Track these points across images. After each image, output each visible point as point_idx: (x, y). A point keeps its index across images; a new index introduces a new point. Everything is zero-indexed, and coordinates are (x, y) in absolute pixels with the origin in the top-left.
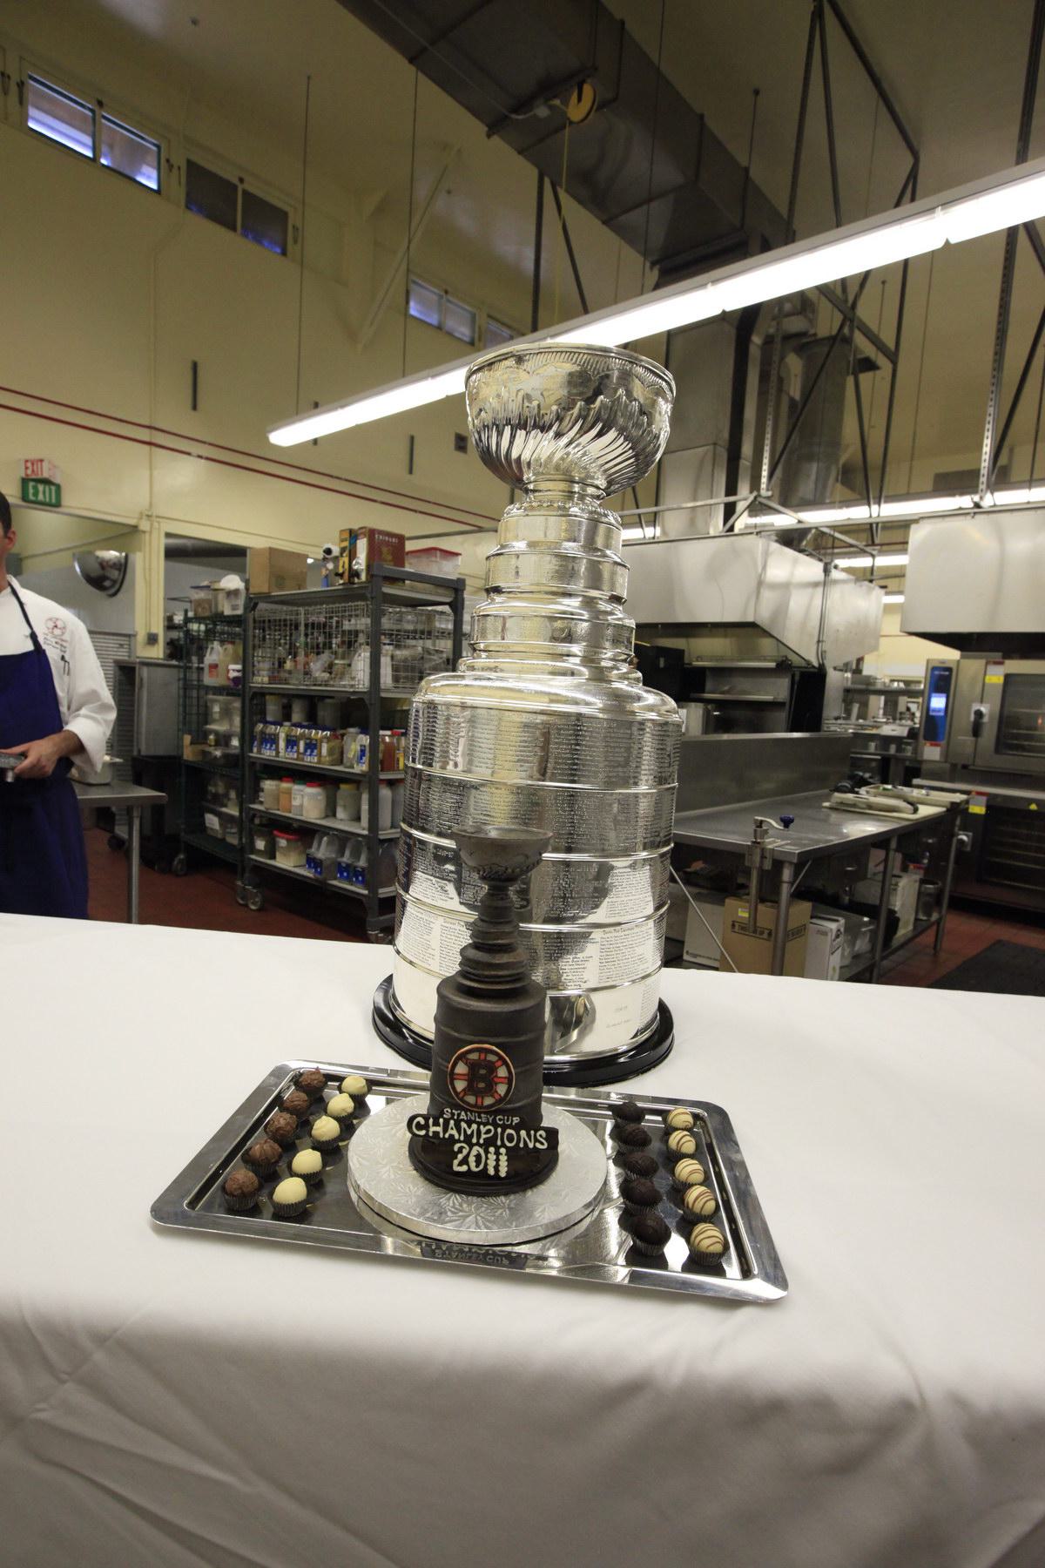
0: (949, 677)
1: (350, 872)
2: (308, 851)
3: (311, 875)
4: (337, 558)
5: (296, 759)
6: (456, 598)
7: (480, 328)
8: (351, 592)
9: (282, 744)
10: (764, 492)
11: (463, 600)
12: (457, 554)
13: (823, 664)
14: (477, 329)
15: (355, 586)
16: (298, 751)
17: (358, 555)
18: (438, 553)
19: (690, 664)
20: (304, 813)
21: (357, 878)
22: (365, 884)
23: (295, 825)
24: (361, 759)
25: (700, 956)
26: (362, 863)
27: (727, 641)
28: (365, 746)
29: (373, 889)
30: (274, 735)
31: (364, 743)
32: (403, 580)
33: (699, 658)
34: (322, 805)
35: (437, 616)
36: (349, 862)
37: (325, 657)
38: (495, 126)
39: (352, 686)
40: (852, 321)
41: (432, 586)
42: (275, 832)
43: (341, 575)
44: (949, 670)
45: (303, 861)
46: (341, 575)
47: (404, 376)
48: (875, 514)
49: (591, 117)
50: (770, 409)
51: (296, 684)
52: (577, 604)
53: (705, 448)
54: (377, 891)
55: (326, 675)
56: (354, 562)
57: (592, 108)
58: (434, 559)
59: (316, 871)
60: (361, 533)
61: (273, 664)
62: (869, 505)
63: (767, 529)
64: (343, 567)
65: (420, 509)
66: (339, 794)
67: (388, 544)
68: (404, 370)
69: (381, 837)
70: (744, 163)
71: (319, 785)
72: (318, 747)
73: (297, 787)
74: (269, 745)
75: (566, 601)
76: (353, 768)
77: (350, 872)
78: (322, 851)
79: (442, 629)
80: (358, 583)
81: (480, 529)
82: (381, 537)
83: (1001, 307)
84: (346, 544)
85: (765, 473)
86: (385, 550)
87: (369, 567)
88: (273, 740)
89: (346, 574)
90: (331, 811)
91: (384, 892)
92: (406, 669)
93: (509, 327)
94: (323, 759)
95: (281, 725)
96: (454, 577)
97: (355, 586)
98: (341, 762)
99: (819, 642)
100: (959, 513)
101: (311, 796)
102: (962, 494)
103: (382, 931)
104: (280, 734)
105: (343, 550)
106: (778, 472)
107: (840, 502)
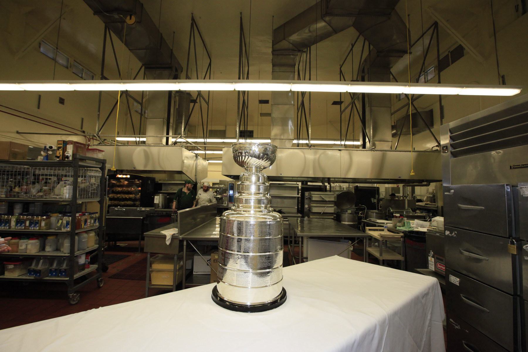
0: (234, 185)
1: (58, 272)
2: (29, 268)
3: (33, 278)
4: (54, 150)
5: (25, 229)
6: (103, 166)
7: (70, 63)
8: (63, 163)
9: (13, 223)
10: (182, 135)
11: (105, 167)
12: (103, 151)
13: (197, 182)
14: (69, 64)
15: (66, 161)
16: (25, 226)
17: (67, 150)
18: (97, 151)
19: (158, 182)
20: (27, 252)
21: (61, 274)
22: (66, 276)
23: (21, 257)
24: (67, 226)
25: (198, 272)
26: (64, 266)
27: (166, 174)
28: (69, 221)
29: (71, 276)
30: (8, 220)
31: (68, 220)
32: (85, 160)
33: (160, 180)
34: (38, 247)
35: (89, 171)
36: (57, 268)
37: (37, 186)
38: (97, 12)
39: (61, 198)
40: (200, 94)
41: (95, 162)
42: (5, 263)
43: (58, 157)
44: (233, 184)
45: (24, 272)
46: (58, 157)
47: (54, 79)
48: (205, 141)
49: (134, 24)
50: (184, 114)
51: (23, 197)
52: (262, 196)
53: (162, 119)
54: (73, 277)
55: (41, 194)
56: (66, 153)
57: (135, 22)
58: (95, 152)
59: (36, 275)
60: (70, 143)
61: (8, 189)
62: (204, 139)
63: (184, 145)
64: (59, 154)
65: (42, 122)
66: (47, 241)
67: (80, 147)
68: (54, 78)
69: (75, 255)
70: (171, 48)
71: (37, 239)
72: (40, 221)
73: (22, 241)
74: (3, 224)
75: (260, 195)
76: (61, 230)
77: (58, 272)
78: (40, 267)
79: (91, 175)
80: (67, 160)
81: (76, 134)
82: (78, 145)
83: (238, 102)
84: (62, 146)
85: (183, 130)
86: (79, 149)
87: (74, 155)
88: (8, 222)
89: (61, 157)
90: (43, 248)
91: (76, 276)
92: (84, 191)
93: (82, 66)
94: (42, 228)
95: (12, 214)
96: (102, 159)
97: (65, 161)
98: (50, 228)
99: (195, 176)
100: (223, 142)
101: (32, 244)
102: (224, 139)
103: (75, 293)
104: (12, 219)
105: (59, 148)
106: (187, 130)
107: (199, 137)
